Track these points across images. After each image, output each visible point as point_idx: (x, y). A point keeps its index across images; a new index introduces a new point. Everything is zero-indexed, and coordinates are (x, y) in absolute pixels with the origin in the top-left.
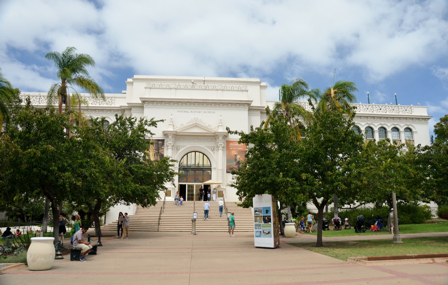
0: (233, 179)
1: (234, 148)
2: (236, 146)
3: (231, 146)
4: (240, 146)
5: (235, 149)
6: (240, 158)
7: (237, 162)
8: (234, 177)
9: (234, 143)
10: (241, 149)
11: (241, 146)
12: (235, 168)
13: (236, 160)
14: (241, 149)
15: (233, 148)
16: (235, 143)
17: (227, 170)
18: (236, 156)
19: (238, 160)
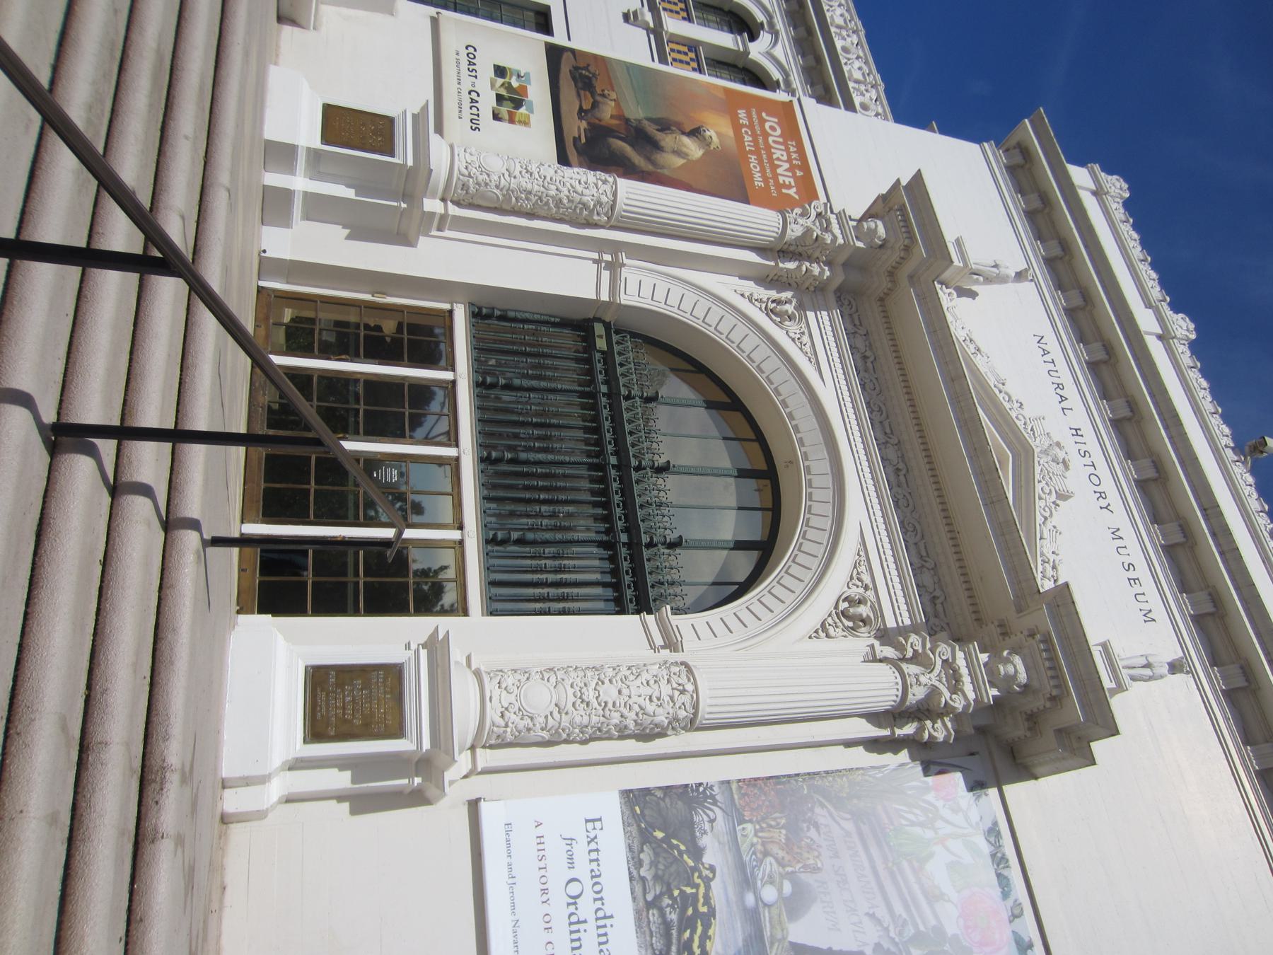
0: (500, 71)
1: (754, 135)
2: (770, 155)
3: (762, 122)
4: (775, 176)
5: (747, 138)
6: (678, 153)
7: (651, 129)
8: (515, 84)
9: (784, 144)
10: (757, 176)
11: (779, 186)
12: (595, 105)
13: (665, 126)
14: (757, 176)
15: (751, 126)
16: (787, 150)
17: (566, 56)
18: (695, 133)
19: (667, 140)
